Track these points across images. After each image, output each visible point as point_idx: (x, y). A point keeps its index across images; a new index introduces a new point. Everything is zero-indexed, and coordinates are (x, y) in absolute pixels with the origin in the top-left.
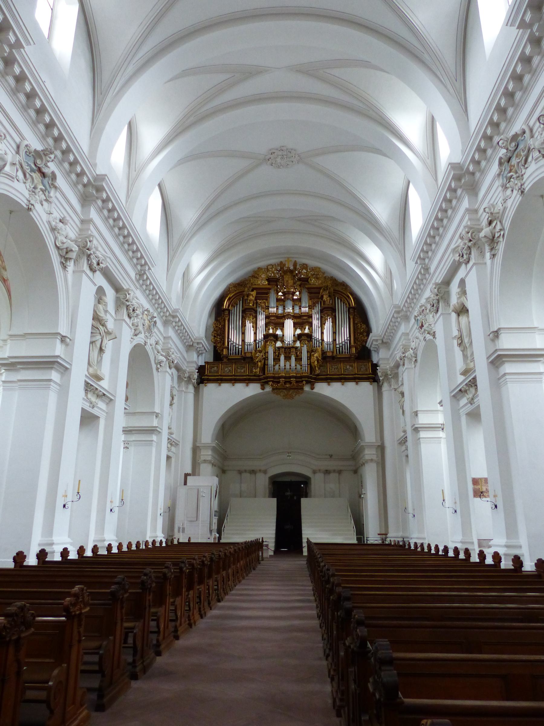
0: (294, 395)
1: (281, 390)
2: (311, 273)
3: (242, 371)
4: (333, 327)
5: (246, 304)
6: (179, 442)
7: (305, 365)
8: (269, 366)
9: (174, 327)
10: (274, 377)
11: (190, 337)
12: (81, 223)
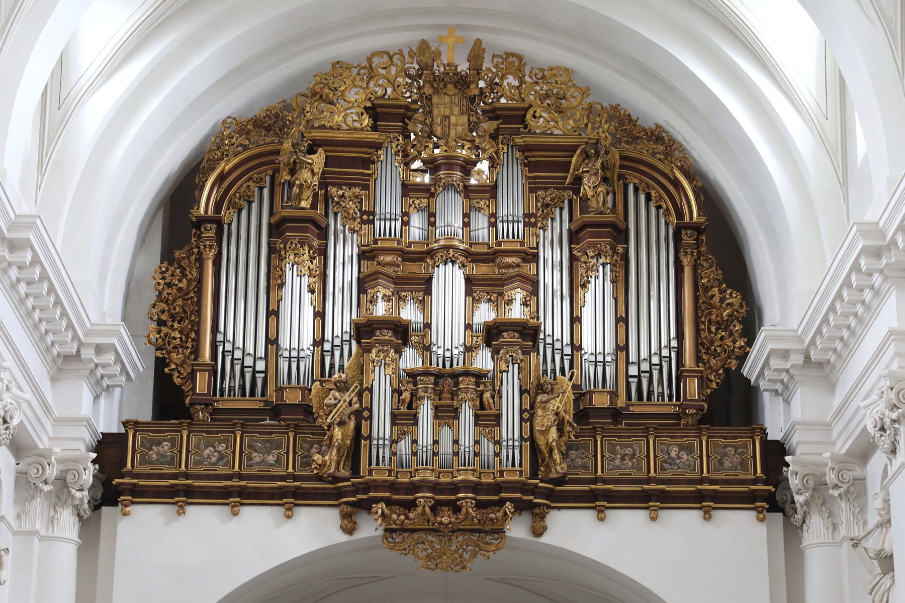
0: (466, 556)
1: (416, 536)
2: (538, 88)
3: (271, 459)
4: (616, 300)
8: (375, 442)
9: (13, 287)
10: (393, 487)
11: (70, 326)
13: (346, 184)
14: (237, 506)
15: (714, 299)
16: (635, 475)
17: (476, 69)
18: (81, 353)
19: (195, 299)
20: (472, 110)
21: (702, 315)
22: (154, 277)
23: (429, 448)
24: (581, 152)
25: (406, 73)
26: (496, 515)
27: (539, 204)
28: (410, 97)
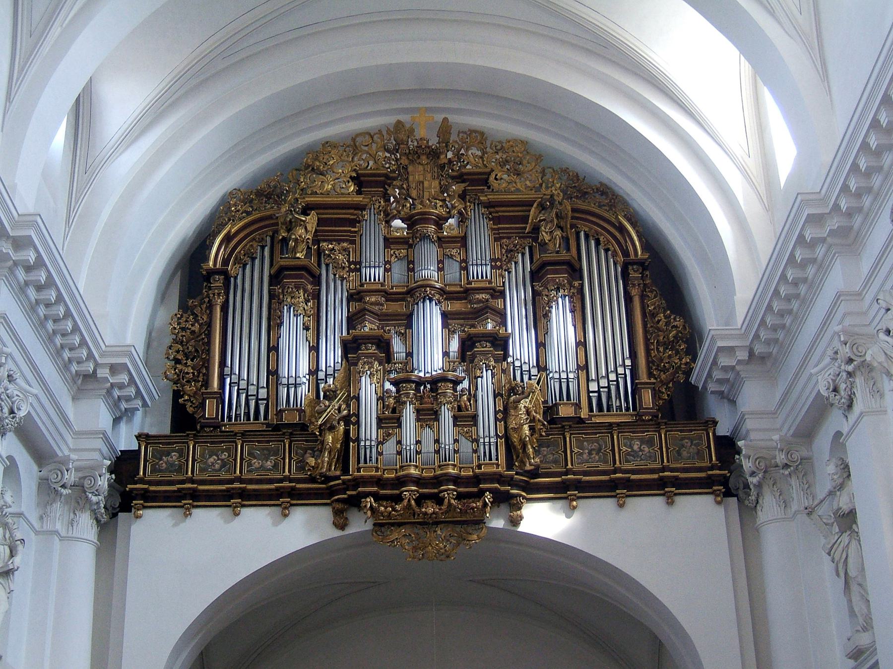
2: (498, 157)
5: (282, 253)
7: (487, 440)
8: (362, 443)
10: (379, 482)
13: (335, 240)
14: (238, 507)
15: (661, 323)
16: (602, 467)
17: (445, 142)
18: (98, 372)
19: (206, 340)
20: (442, 176)
21: (651, 338)
22: (170, 324)
23: (412, 447)
24: (538, 205)
25: (385, 148)
26: (476, 504)
27: (504, 251)
28: (389, 168)
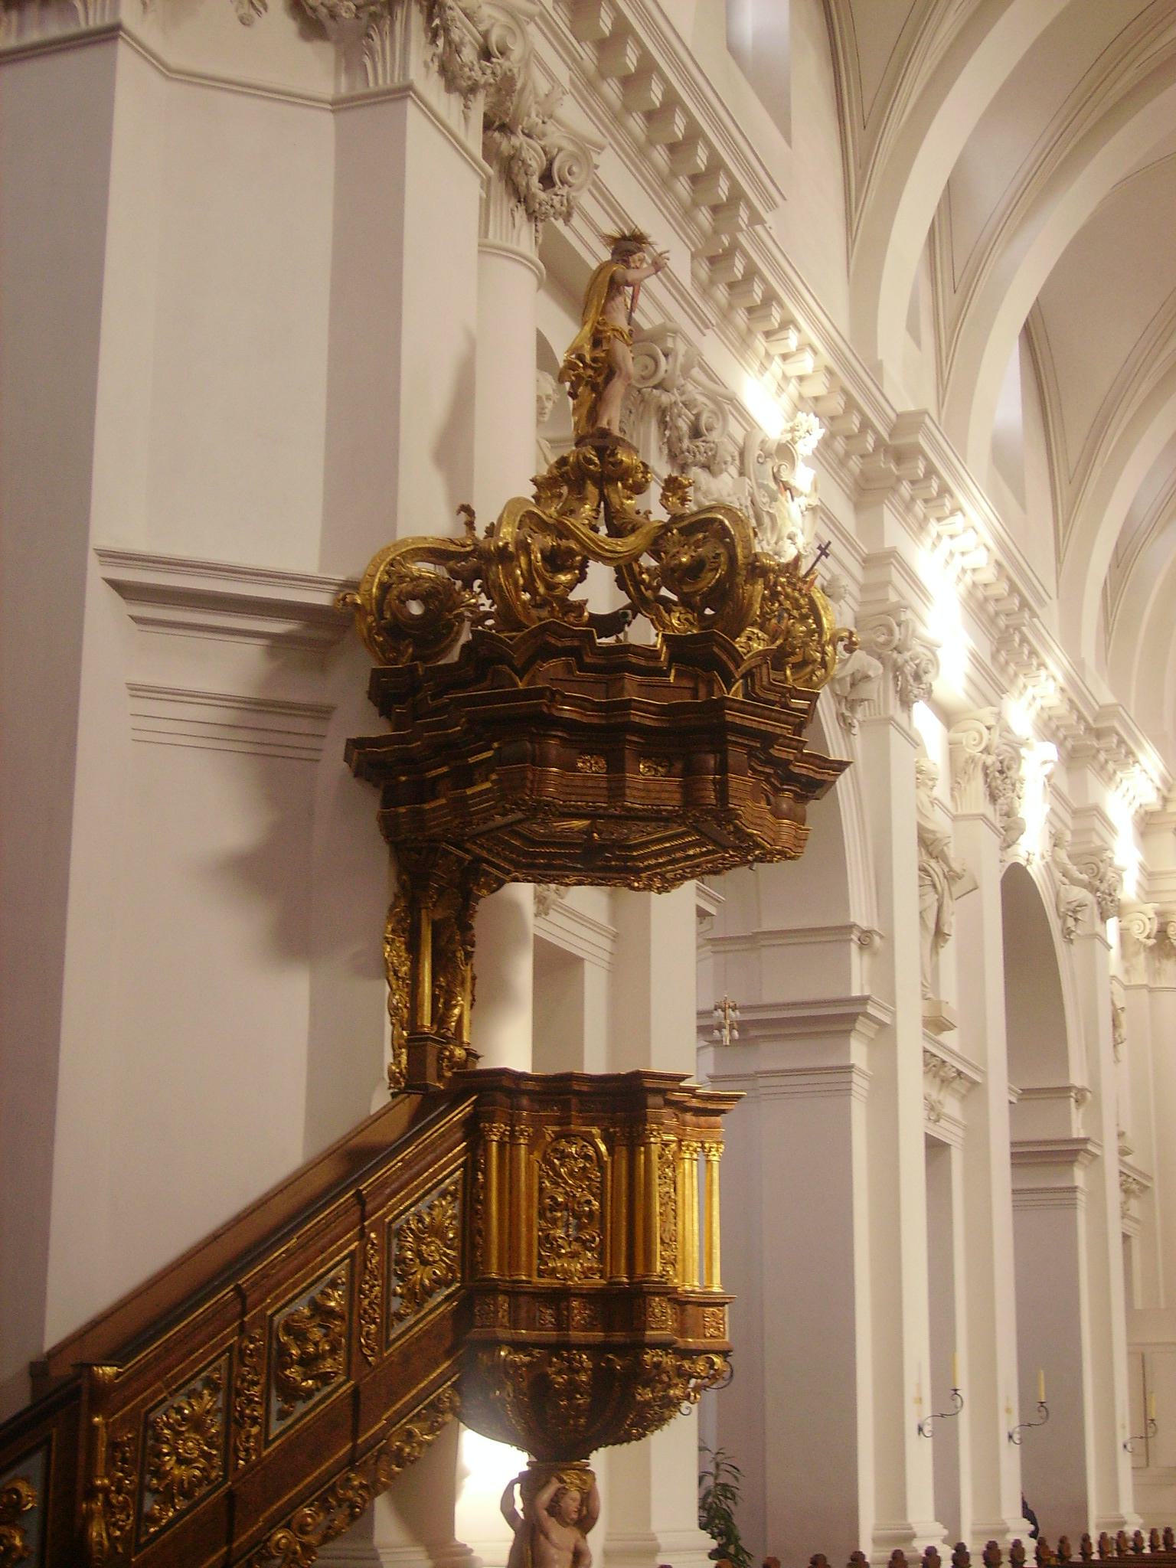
6: (1150, 1178)
12: (863, 568)
